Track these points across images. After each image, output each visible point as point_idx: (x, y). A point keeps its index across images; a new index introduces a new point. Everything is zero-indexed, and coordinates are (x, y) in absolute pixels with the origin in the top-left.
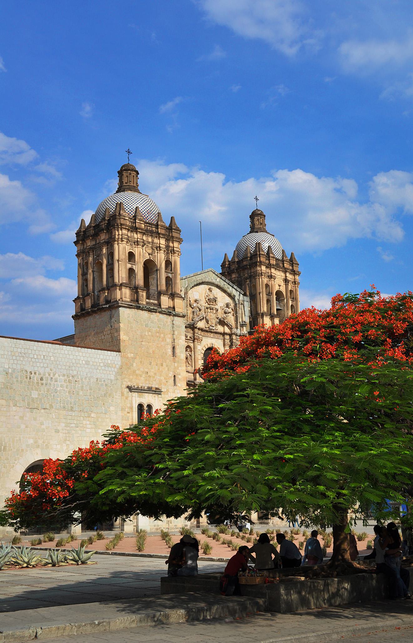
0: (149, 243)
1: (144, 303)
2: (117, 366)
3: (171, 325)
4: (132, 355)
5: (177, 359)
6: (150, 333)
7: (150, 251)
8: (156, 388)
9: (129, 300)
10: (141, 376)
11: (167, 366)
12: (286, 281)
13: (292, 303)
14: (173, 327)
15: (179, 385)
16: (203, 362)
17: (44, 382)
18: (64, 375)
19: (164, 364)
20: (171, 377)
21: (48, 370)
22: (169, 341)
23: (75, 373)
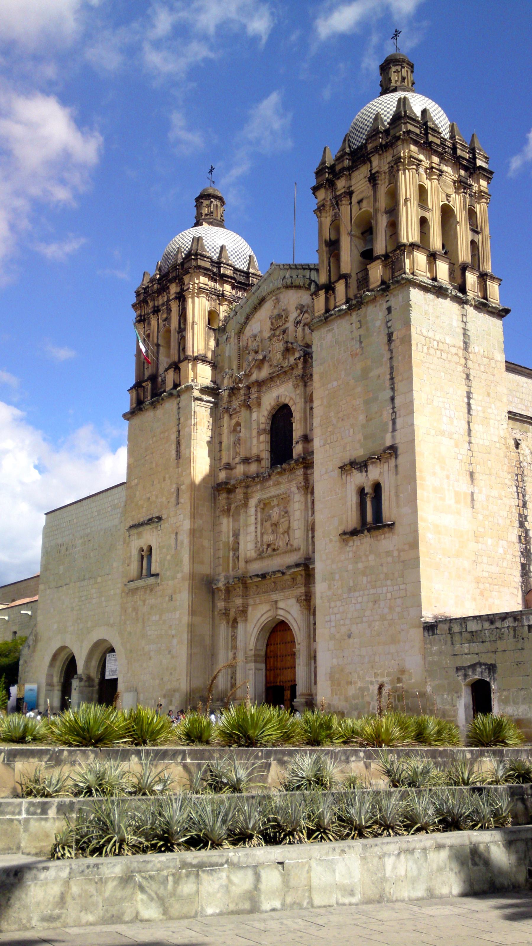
0: (163, 305)
1: (149, 398)
2: (122, 505)
3: (176, 413)
4: (136, 481)
5: (181, 461)
6: (154, 438)
7: (165, 316)
8: (157, 518)
9: (135, 405)
10: (143, 508)
11: (170, 478)
12: (373, 179)
13: (390, 216)
14: (179, 413)
15: (182, 500)
16: (263, 438)
17: (68, 552)
18: (81, 537)
19: (167, 476)
20: (173, 493)
21: (71, 536)
22: (173, 437)
23: (89, 531)
